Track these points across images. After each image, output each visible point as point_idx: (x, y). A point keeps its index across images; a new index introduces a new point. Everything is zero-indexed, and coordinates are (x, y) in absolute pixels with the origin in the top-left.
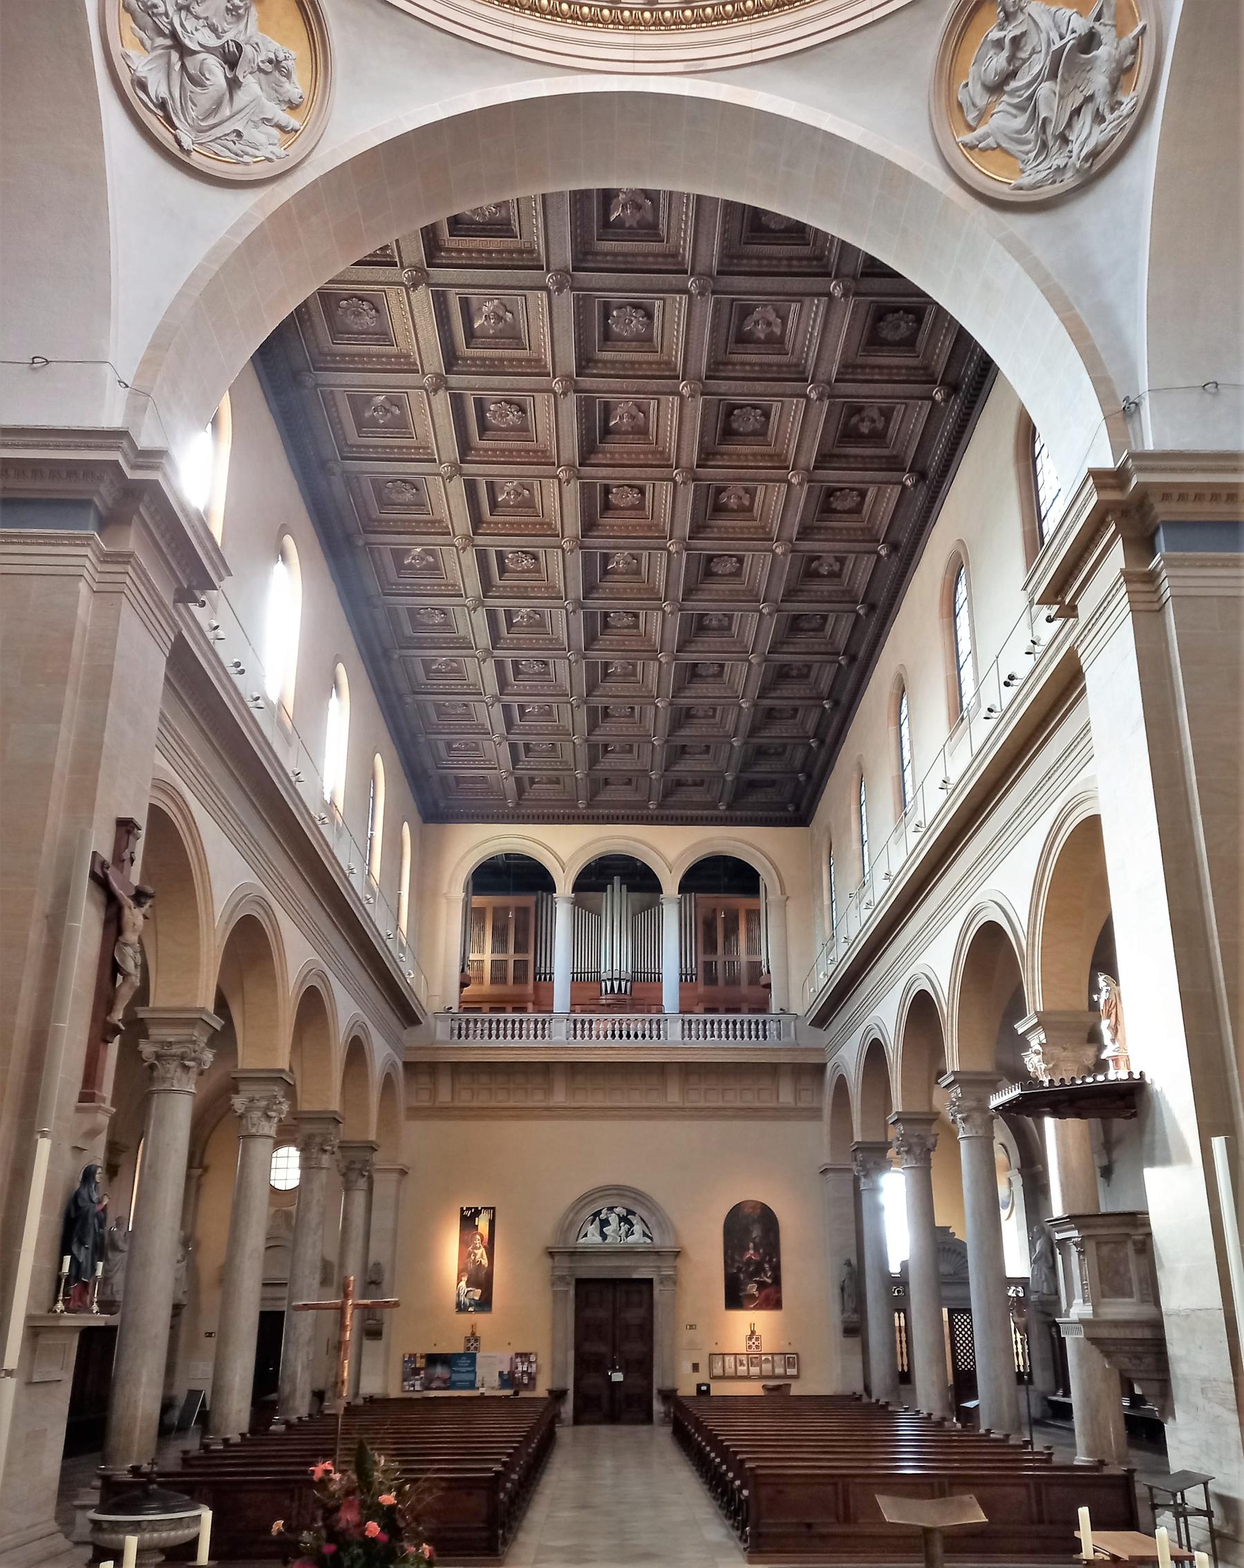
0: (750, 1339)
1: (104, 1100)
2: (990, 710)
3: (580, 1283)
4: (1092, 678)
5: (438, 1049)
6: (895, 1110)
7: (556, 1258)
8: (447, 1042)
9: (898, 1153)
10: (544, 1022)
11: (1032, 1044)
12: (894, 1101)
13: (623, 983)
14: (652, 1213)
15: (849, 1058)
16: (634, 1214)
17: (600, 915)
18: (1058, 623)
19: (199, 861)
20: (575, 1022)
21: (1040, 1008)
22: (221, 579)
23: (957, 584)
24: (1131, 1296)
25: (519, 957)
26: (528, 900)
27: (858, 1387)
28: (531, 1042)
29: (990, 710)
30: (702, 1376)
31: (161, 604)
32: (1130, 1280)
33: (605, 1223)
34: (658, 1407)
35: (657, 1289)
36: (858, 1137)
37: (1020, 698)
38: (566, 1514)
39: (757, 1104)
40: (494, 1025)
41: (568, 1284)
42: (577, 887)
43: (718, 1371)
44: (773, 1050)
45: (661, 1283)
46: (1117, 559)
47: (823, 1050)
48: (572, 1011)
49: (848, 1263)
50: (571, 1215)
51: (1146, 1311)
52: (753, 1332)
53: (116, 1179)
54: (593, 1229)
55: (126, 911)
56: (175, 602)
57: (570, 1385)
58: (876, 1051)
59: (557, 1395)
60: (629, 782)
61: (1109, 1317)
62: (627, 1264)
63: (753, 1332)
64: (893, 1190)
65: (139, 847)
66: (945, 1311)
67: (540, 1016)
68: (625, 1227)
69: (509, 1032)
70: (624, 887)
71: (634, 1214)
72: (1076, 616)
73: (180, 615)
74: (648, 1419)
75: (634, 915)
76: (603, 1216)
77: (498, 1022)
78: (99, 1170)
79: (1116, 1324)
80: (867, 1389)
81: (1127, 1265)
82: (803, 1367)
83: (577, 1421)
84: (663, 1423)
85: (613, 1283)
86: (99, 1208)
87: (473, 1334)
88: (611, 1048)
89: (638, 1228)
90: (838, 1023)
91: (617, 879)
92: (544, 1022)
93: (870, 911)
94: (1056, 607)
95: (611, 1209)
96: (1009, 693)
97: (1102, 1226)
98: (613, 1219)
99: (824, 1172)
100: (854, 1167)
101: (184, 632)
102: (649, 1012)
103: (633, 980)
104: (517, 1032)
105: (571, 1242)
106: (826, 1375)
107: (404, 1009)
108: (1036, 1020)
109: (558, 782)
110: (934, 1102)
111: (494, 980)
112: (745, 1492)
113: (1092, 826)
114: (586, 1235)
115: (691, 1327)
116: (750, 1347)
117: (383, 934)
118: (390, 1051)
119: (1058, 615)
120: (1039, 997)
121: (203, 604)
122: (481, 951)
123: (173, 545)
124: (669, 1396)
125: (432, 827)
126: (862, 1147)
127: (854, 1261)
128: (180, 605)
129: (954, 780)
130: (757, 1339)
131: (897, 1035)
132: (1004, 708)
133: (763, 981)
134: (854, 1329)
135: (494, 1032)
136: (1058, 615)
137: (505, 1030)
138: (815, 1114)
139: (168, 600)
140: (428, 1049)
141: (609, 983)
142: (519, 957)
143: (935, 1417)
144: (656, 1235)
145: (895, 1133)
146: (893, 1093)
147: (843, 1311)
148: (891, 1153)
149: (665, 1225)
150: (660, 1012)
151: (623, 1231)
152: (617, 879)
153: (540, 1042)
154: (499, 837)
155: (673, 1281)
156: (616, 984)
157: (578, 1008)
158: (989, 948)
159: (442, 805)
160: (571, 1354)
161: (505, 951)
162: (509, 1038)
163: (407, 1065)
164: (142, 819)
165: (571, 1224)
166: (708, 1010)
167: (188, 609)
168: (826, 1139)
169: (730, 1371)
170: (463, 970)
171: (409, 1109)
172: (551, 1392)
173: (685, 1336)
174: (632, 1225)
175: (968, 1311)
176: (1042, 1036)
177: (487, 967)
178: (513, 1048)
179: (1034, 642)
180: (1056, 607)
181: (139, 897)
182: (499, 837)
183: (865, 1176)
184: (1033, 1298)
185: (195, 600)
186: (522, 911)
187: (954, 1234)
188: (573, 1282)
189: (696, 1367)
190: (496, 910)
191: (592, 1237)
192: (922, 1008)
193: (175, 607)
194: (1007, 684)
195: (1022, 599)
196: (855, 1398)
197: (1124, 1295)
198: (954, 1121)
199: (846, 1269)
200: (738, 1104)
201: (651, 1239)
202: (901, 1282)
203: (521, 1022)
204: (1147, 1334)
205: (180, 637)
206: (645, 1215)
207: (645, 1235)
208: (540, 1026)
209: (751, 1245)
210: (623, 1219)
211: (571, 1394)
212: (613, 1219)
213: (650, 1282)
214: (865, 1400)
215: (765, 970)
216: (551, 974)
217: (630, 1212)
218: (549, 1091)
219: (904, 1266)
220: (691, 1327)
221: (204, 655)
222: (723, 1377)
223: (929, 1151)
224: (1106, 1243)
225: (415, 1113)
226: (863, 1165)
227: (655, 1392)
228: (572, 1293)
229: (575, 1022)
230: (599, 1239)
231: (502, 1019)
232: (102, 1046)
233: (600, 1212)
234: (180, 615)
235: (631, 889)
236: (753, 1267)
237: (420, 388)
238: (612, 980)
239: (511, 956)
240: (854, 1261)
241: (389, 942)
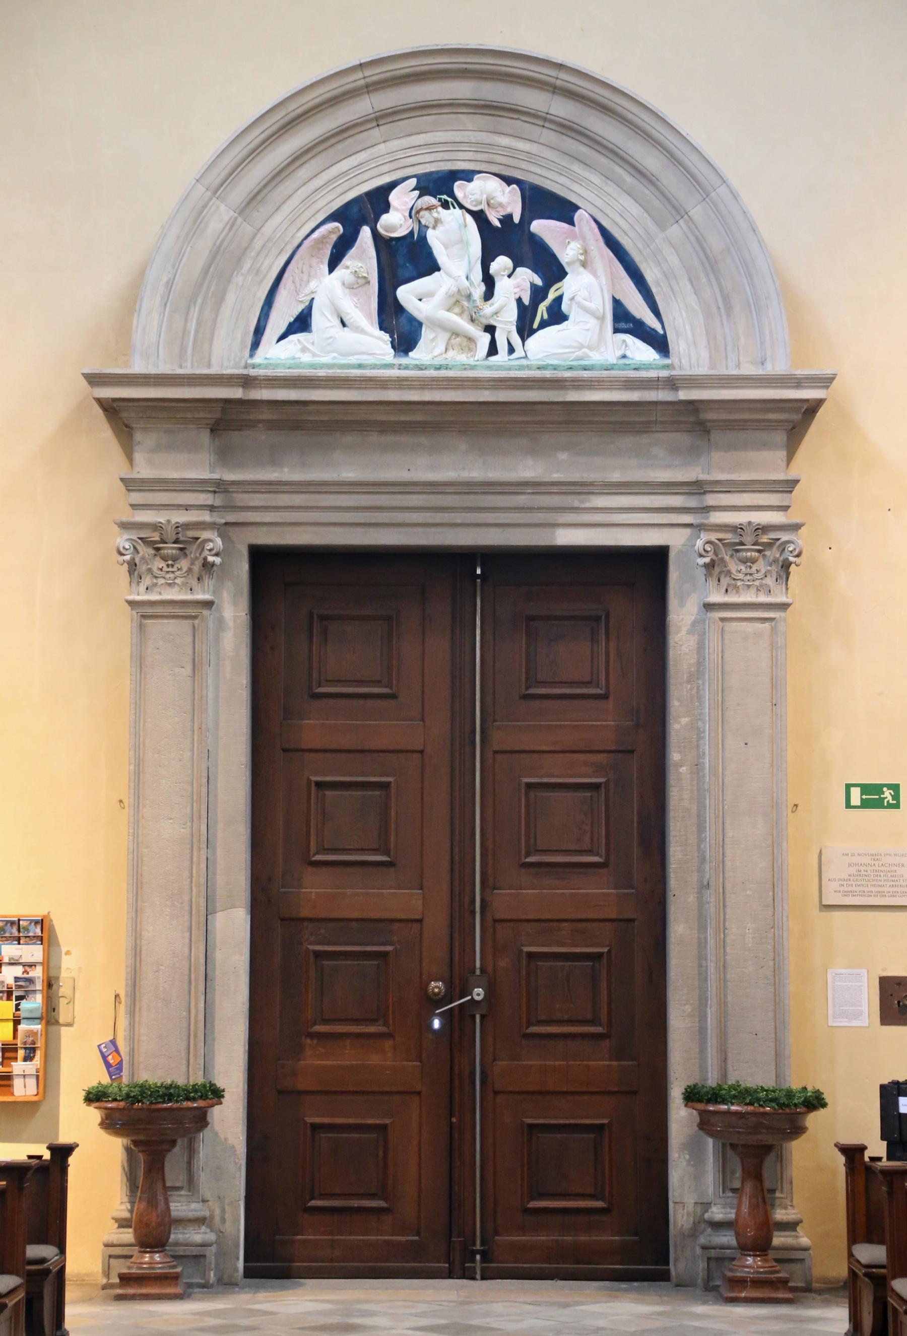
7: (145, 439)
16: (564, 210)
33: (408, 258)
50: (221, 214)
57: (231, 1072)
62: (528, 469)
68: (515, 282)
71: (564, 210)
76: (395, 221)
95: (439, 186)
105: (225, 354)
114: (302, 323)
115: (875, 797)
144: (681, 320)
151: (504, 310)
160: (234, 925)
165: (222, 264)
174: (552, 270)
188: (244, 567)
201: (660, 344)
207: (623, 321)
210: (501, 239)
211: (229, 1122)
213: (657, 558)
217: (544, 202)
220: (875, 797)
230: (373, 346)
233: (378, 200)
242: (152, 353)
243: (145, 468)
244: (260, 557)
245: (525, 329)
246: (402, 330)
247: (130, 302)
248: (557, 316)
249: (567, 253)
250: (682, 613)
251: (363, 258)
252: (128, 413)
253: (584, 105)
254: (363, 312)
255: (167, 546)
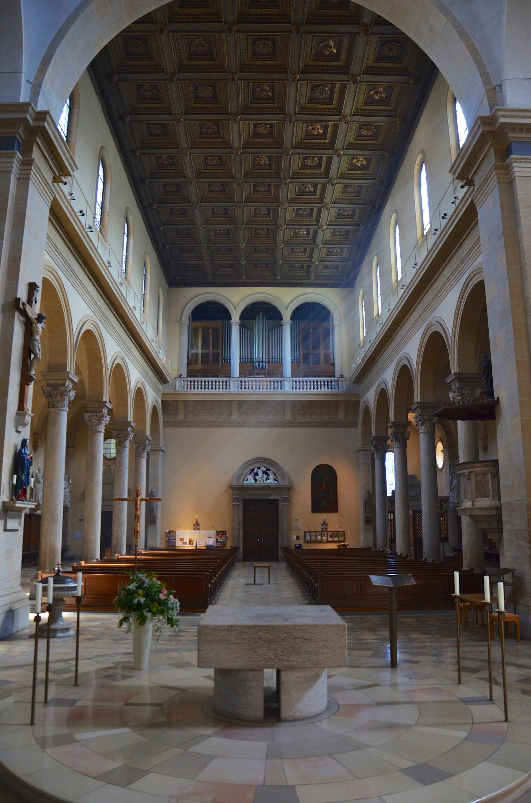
0: (323, 525)
1: (28, 410)
2: (436, 230)
3: (244, 500)
4: (482, 213)
5: (177, 394)
6: (391, 421)
8: (182, 391)
9: (392, 441)
10: (226, 382)
11: (453, 387)
12: (391, 417)
13: (264, 364)
14: (278, 470)
15: (371, 397)
16: (270, 470)
17: (253, 331)
18: (466, 188)
19: (66, 304)
20: (241, 382)
21: (456, 371)
22: (73, 171)
23: (421, 170)
24: (489, 497)
25: (215, 351)
26: (218, 324)
27: (372, 545)
28: (221, 391)
29: (436, 230)
30: (301, 541)
31: (46, 183)
32: (489, 490)
33: (256, 474)
34: (281, 553)
35: (280, 504)
36: (374, 434)
37: (449, 224)
38: (238, 594)
39: (327, 420)
40: (203, 383)
41: (239, 501)
42: (242, 318)
43: (308, 538)
44: (335, 395)
45: (283, 501)
46: (491, 160)
47: (359, 395)
48: (240, 377)
49: (368, 492)
51: (496, 503)
52: (324, 522)
53: (37, 451)
54: (250, 477)
55: (34, 325)
56: (53, 182)
58: (383, 394)
59: (235, 549)
60: (267, 266)
61: (479, 506)
62: (267, 492)
63: (324, 522)
64: (390, 458)
65: (38, 296)
66: (411, 512)
67: (225, 379)
68: (265, 476)
69: (210, 386)
70: (264, 318)
72: (474, 185)
73: (55, 189)
74: (276, 559)
75: (269, 331)
76: (255, 471)
77: (205, 382)
78: (28, 441)
79: (481, 509)
80: (375, 545)
81: (488, 484)
82: (346, 536)
83: (245, 560)
84: (283, 561)
85: (260, 501)
86: (29, 457)
87: (197, 523)
88: (258, 394)
89: (271, 477)
90: (366, 381)
91: (261, 314)
92: (226, 382)
93: (381, 327)
94: (465, 181)
95: (259, 468)
96: (444, 221)
97: (478, 467)
98: (260, 472)
99: (357, 451)
100: (372, 448)
101: (57, 197)
102: (277, 377)
103: (269, 362)
104: (214, 386)
106: (356, 540)
107: (160, 376)
108: (454, 377)
109: (232, 266)
110: (409, 417)
111: (203, 362)
112: (316, 585)
113: (481, 284)
114: (247, 480)
115: (296, 521)
116: (323, 529)
117: (150, 339)
118: (156, 395)
119: (466, 185)
120: (456, 366)
121: (65, 183)
122: (197, 348)
123: (52, 156)
124: (286, 550)
125: (174, 289)
126: (376, 439)
127: (371, 491)
128: (55, 184)
129: (419, 264)
130: (326, 525)
131: (393, 386)
132: (442, 229)
133: (331, 362)
134: (369, 521)
135: (203, 386)
136: (466, 185)
137: (208, 385)
138: (355, 425)
139: (50, 180)
140: (173, 394)
141: (257, 364)
142: (215, 351)
143: (404, 555)
144: (279, 479)
145: (390, 431)
146: (390, 411)
147: (365, 513)
148: (389, 442)
149: (283, 475)
150: (282, 377)
152: (261, 314)
153: (225, 391)
154: (204, 294)
155: (288, 500)
156: (261, 364)
157: (242, 375)
158: (435, 344)
159: (178, 278)
160: (241, 531)
161: (208, 348)
162: (210, 389)
163: (162, 401)
164: (40, 284)
165: (241, 475)
166: (304, 376)
167: (59, 185)
168: (359, 436)
169: (313, 538)
170: (188, 357)
171: (164, 422)
172: (232, 547)
173: (294, 525)
174: (269, 475)
175: (420, 512)
176: (457, 384)
177: (200, 355)
178: (212, 394)
179: (455, 197)
180: (465, 181)
181: (40, 318)
182: (204, 294)
183: (377, 452)
184: (451, 505)
185: (62, 182)
186: (215, 329)
187: (417, 478)
189: (298, 538)
190: (203, 329)
191: (250, 481)
192: (404, 373)
193: (53, 185)
194: (443, 218)
195: (450, 177)
196: (369, 549)
197: (485, 497)
198: (417, 425)
199: (367, 495)
200: (319, 420)
201: (278, 481)
202: (392, 500)
203: (216, 382)
204: (494, 512)
205: (55, 199)
206: (274, 470)
207: (275, 480)
208: (225, 384)
209: (324, 484)
210: (264, 473)
211: (241, 548)
212: (260, 472)
213: (278, 500)
214: (374, 549)
215: (332, 357)
216: (230, 359)
218: (230, 414)
219: (393, 492)
221: (66, 207)
222: (311, 542)
223: (406, 440)
224: (479, 475)
225: (166, 424)
226: (376, 447)
227: (279, 548)
228: (241, 505)
229: (241, 382)
230: (254, 482)
231: (207, 381)
232: (26, 386)
233: (254, 469)
234: (55, 189)
235: (268, 319)
236: (325, 492)
237: (166, 80)
238: (259, 362)
239: (211, 351)
240: (371, 491)
241: (153, 343)
242: (235, 483)
243: (234, 493)
244: (244, 500)
245: (266, 480)
246: (256, 480)
247: (233, 477)
248: (269, 479)
249: (270, 474)
250: (280, 505)
251: (252, 474)
252: (233, 488)
253: (272, 463)
254: (252, 479)
255: (236, 499)
